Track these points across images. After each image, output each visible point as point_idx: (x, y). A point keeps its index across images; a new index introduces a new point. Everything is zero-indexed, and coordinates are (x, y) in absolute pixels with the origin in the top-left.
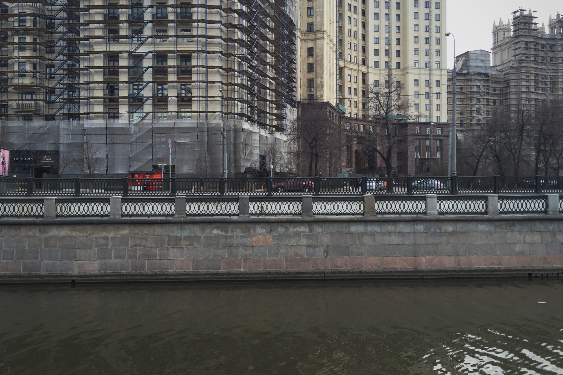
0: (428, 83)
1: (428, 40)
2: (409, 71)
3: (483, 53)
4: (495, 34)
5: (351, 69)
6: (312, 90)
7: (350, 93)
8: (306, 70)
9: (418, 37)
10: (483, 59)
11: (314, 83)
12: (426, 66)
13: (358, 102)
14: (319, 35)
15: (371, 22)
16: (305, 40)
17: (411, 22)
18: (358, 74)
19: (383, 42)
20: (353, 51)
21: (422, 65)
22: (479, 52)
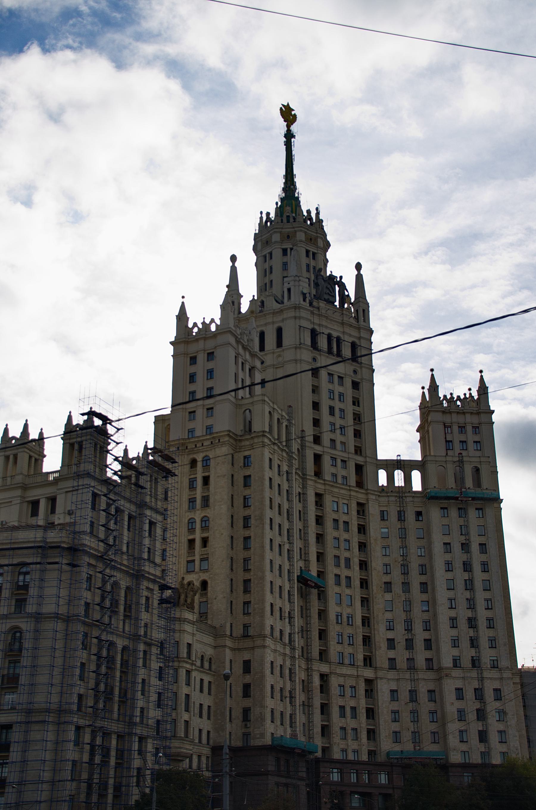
0: (479, 694)
5: (344, 676)
6: (248, 726)
7: (343, 715)
8: (241, 694)
9: (456, 619)
11: (252, 714)
12: (474, 665)
13: (359, 731)
14: (259, 642)
16: (239, 649)
18: (357, 683)
21: (466, 662)
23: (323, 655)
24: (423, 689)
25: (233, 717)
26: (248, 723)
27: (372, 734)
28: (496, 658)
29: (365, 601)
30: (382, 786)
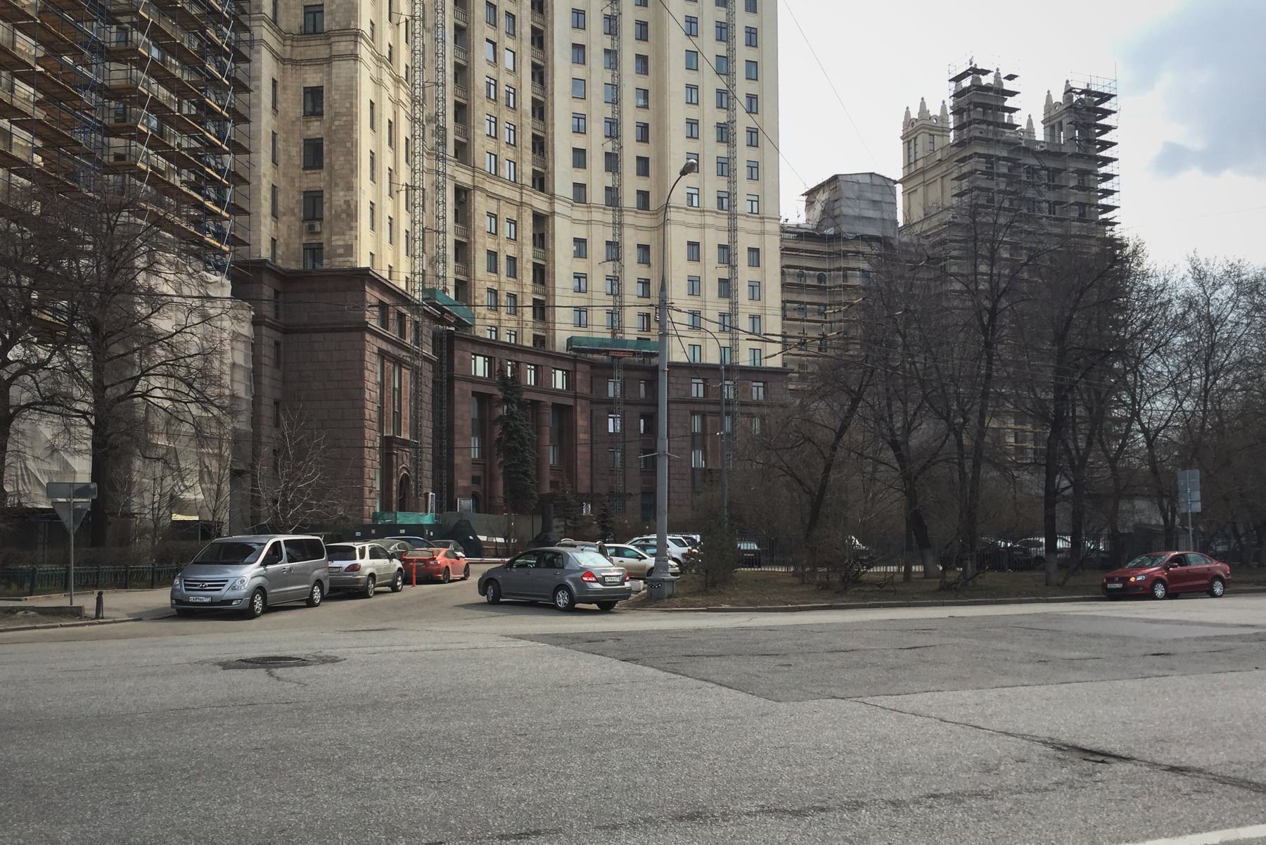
0: (726, 253)
1: (725, 133)
2: (673, 215)
3: (877, 181)
4: (909, 142)
5: (498, 198)
6: (318, 228)
7: (493, 267)
8: (298, 161)
10: (878, 198)
11: (326, 206)
12: (721, 206)
14: (342, 46)
15: (562, 70)
16: (295, 63)
17: (677, 77)
18: (520, 215)
19: (597, 129)
20: (503, 145)
21: (710, 202)
22: (867, 180)
23: (463, 152)
24: (631, 240)
25: (281, 208)
26: (317, 224)
27: (541, 309)
28: (756, 198)
29: (540, 74)
30: (557, 393)
